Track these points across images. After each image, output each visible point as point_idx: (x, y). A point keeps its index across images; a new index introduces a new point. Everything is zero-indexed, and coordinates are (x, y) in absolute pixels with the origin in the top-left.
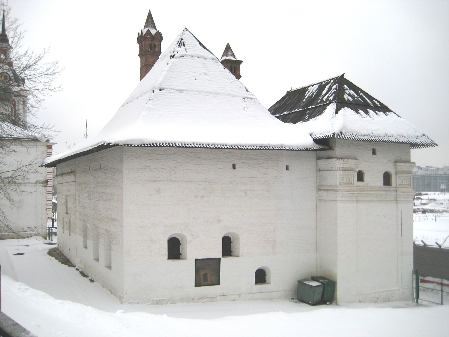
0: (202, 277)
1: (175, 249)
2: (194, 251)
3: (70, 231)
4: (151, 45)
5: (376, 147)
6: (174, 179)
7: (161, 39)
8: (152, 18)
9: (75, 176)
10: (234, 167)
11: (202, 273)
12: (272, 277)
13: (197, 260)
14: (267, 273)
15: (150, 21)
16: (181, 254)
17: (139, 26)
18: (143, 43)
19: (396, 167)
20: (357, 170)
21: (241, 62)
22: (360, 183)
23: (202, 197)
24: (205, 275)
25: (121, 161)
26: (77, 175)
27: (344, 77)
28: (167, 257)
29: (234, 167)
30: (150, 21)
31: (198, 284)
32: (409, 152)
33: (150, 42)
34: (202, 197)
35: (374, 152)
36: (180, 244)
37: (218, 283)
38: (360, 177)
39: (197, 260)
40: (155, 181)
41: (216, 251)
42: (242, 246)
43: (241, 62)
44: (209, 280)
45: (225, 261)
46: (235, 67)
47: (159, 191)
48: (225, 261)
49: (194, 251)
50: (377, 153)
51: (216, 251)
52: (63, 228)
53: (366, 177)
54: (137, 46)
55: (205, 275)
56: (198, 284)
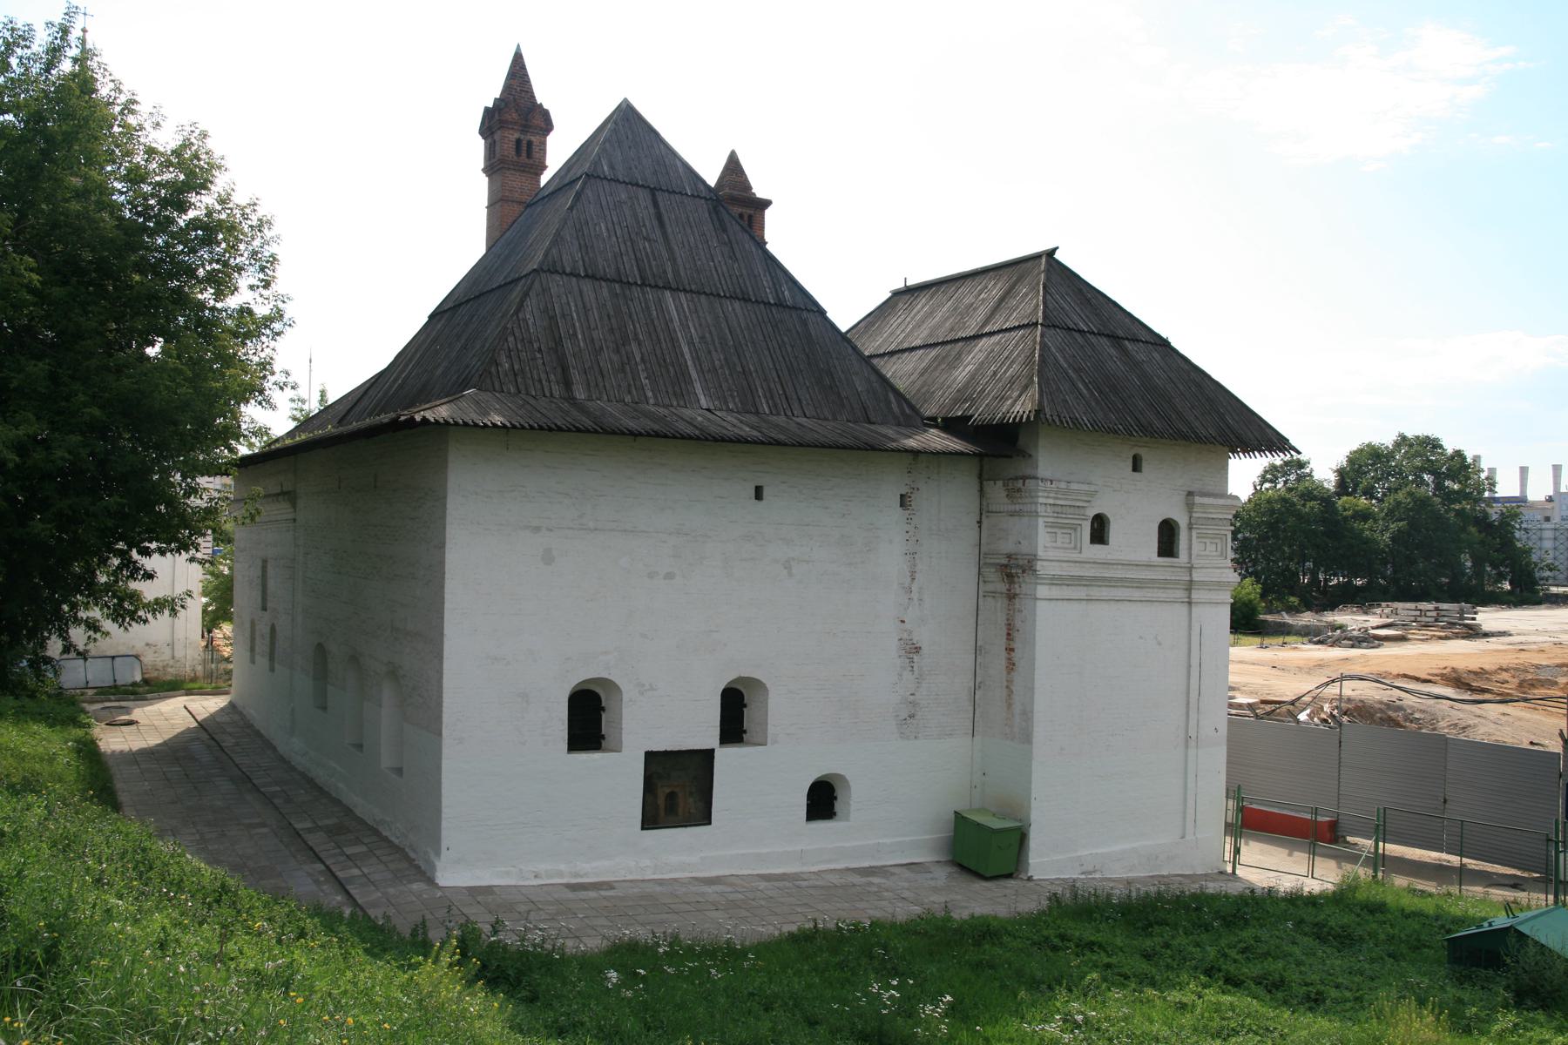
0: (661, 801)
1: (588, 720)
3: (272, 659)
4: (518, 142)
5: (1142, 452)
6: (591, 525)
7: (547, 126)
8: (523, 67)
9: (294, 506)
10: (759, 493)
11: (662, 792)
12: (855, 800)
13: (650, 757)
14: (839, 793)
16: (603, 737)
17: (491, 89)
18: (497, 137)
19: (1190, 506)
20: (1091, 513)
21: (766, 204)
22: (1098, 551)
23: (669, 576)
24: (671, 796)
25: (443, 466)
26: (301, 503)
27: (1057, 256)
28: (564, 744)
29: (759, 493)
30: (518, 72)
31: (652, 819)
32: (1225, 468)
33: (517, 135)
34: (669, 576)
35: (1136, 467)
36: (603, 709)
37: (706, 819)
39: (650, 757)
40: (537, 529)
41: (702, 731)
43: (766, 204)
44: (680, 811)
45: (726, 758)
46: (750, 217)
47: (548, 558)
48: (726, 758)
50: (1145, 466)
51: (702, 731)
52: (252, 650)
53: (1114, 532)
54: (479, 145)
55: (671, 796)
56: (652, 819)
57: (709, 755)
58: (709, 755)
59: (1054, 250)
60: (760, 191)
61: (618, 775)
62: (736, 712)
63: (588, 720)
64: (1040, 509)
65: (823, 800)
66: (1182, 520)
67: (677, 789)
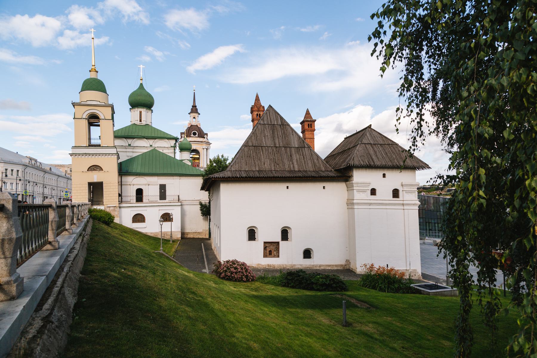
0: (268, 252)
1: (252, 234)
2: (262, 236)
12: (314, 254)
13: (265, 243)
15: (257, 99)
21: (315, 120)
22: (373, 197)
24: (270, 251)
27: (372, 127)
30: (257, 99)
31: (265, 256)
38: (373, 192)
39: (265, 243)
42: (292, 234)
45: (283, 244)
48: (283, 244)
49: (262, 236)
50: (387, 176)
51: (278, 237)
55: (270, 251)
56: (265, 256)
57: (278, 243)
58: (278, 243)
59: (371, 125)
60: (314, 118)
61: (258, 246)
62: (285, 234)
63: (252, 234)
64: (355, 188)
65: (307, 254)
66: (400, 189)
67: (271, 249)
